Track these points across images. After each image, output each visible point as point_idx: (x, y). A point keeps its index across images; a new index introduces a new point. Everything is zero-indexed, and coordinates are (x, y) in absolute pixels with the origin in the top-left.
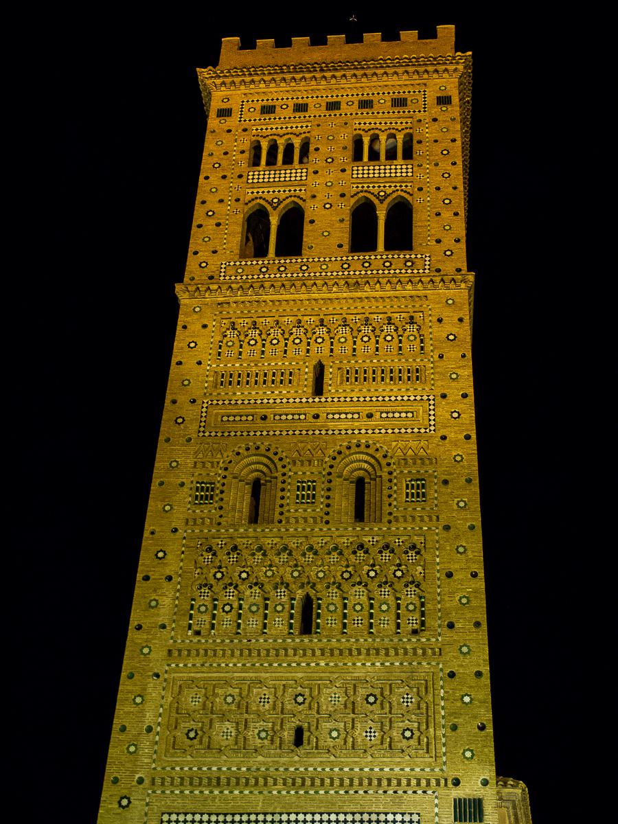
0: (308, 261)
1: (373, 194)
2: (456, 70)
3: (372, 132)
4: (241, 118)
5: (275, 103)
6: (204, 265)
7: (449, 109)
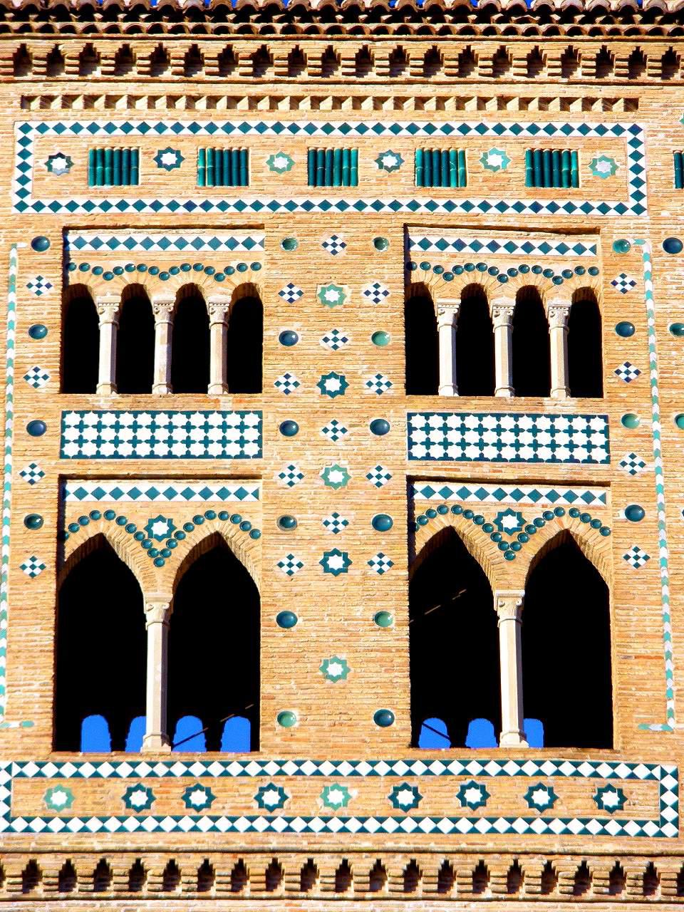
1: (478, 520)
3: (465, 280)
5: (145, 144)
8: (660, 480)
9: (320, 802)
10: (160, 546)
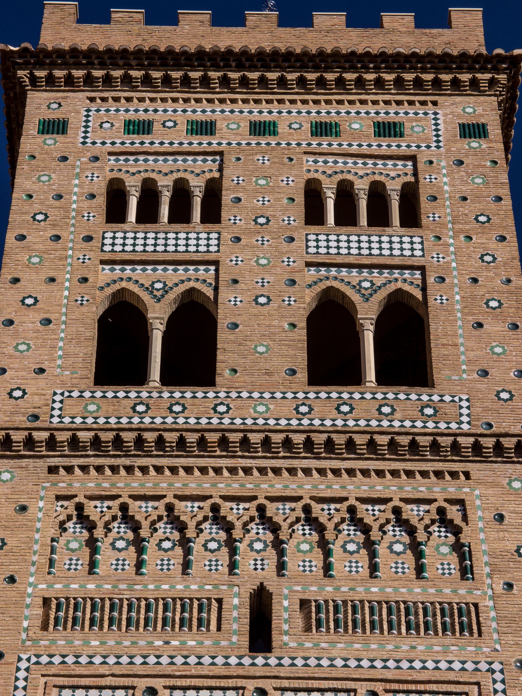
0: (228, 397)
2: (492, 82)
3: (339, 177)
4: (85, 137)
6: (17, 394)
7: (484, 146)
8: (454, 265)
9: (252, 411)
10: (159, 294)
